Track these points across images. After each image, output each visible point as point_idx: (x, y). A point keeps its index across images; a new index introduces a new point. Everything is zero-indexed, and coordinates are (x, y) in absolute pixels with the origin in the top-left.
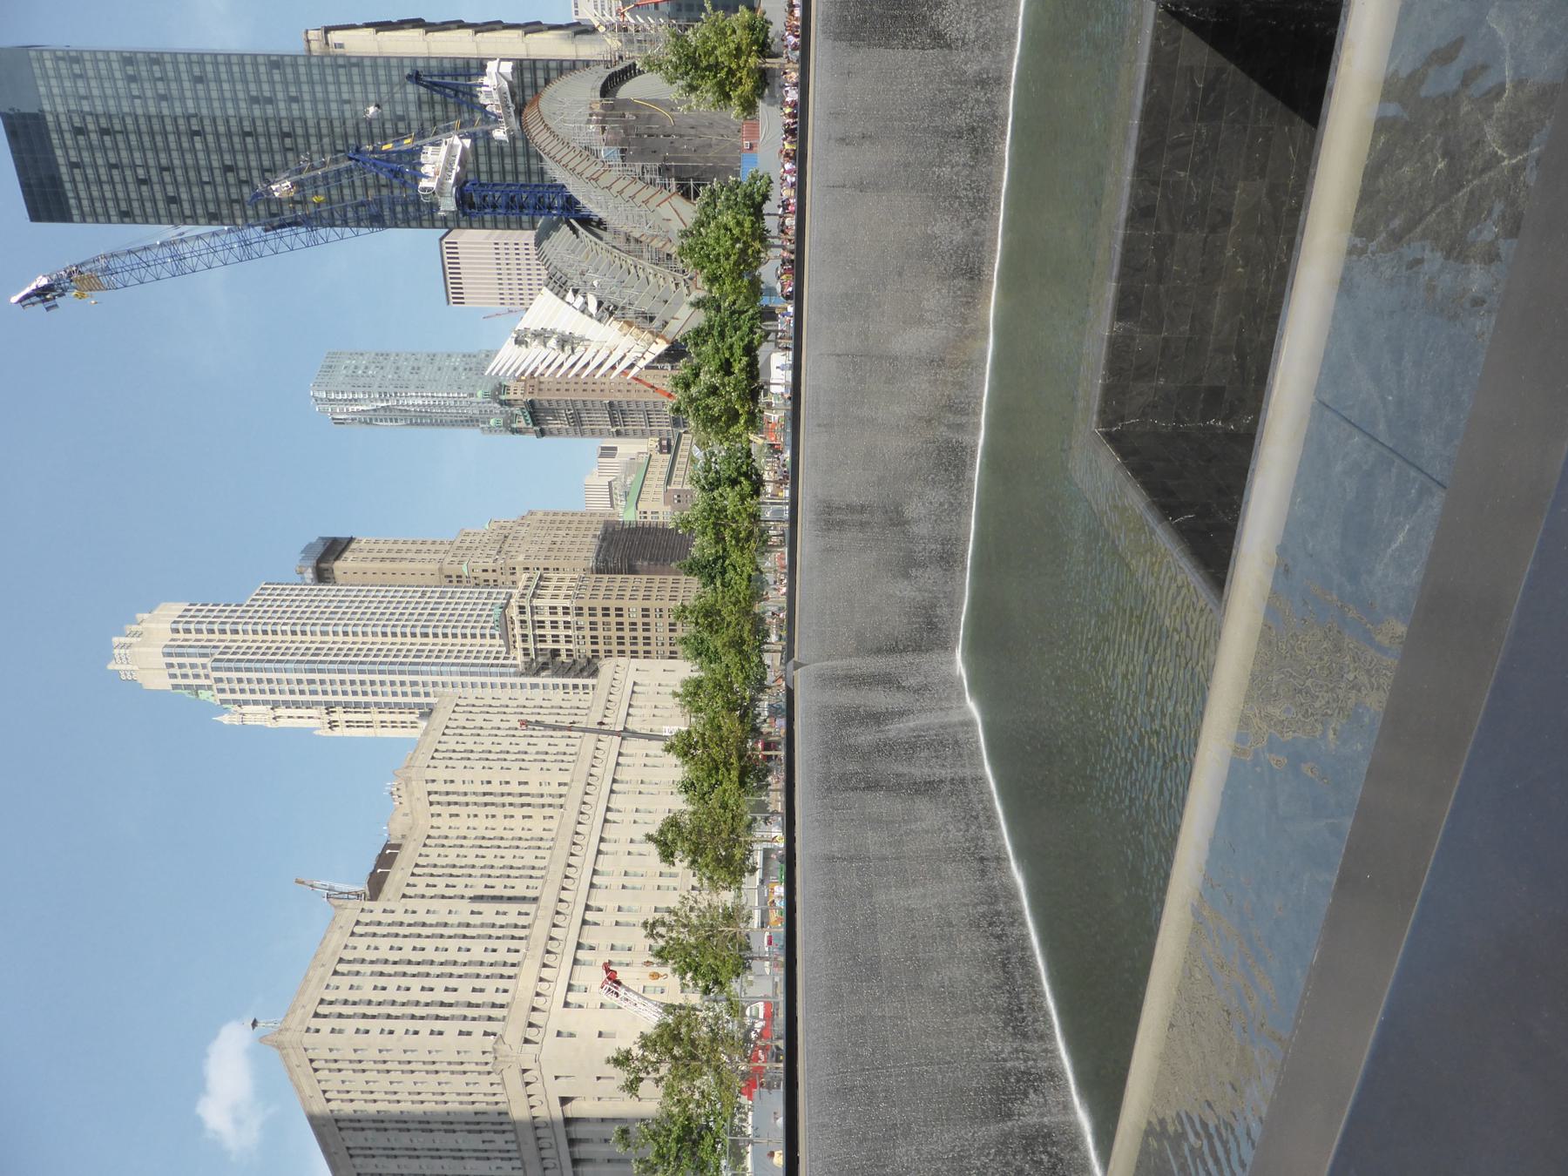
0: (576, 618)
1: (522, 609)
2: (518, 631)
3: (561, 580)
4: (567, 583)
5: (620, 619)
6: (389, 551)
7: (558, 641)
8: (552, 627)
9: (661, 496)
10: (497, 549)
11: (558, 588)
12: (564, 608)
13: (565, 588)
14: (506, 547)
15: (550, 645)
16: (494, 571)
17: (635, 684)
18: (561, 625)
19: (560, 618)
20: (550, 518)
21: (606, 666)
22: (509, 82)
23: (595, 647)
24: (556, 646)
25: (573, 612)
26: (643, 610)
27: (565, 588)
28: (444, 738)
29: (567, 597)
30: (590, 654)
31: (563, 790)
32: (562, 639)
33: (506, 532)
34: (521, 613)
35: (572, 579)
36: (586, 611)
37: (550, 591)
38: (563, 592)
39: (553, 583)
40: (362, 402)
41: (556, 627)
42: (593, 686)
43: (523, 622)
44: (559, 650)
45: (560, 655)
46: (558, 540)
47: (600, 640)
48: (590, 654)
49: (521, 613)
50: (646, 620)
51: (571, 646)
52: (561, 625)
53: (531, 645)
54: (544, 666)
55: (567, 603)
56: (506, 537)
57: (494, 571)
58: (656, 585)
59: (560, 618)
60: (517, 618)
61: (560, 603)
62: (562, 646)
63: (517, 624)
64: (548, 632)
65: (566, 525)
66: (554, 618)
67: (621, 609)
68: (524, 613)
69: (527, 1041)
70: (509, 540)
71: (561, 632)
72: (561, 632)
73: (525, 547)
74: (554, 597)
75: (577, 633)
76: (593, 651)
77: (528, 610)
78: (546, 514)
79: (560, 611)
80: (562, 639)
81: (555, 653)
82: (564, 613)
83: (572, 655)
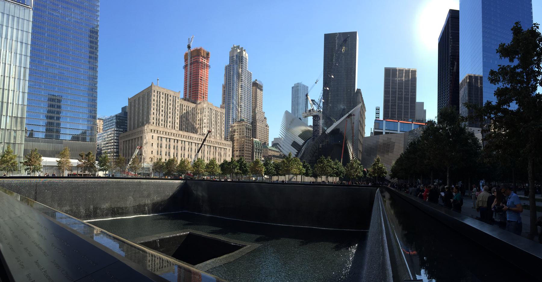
1: (243, 125)
6: (260, 98)
9: (271, 154)
14: (260, 121)
17: (226, 149)
20: (267, 130)
21: (230, 143)
26: (243, 150)
28: (215, 111)
33: (264, 121)
44: (235, 133)
50: (241, 151)
56: (263, 121)
58: (249, 153)
69: (151, 130)
70: (262, 122)
73: (261, 125)
74: (246, 132)
78: (268, 130)
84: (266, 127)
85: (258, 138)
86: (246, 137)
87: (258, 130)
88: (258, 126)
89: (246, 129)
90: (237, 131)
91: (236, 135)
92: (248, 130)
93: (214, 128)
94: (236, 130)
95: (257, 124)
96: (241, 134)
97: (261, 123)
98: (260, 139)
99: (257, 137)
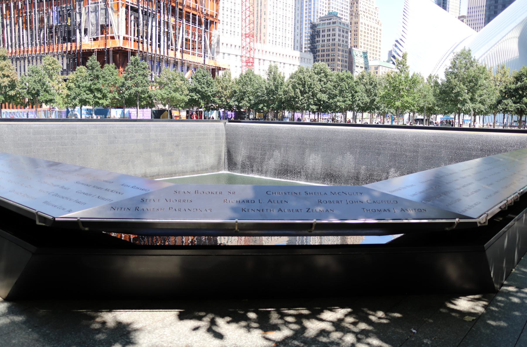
0: (321, 44)
1: (334, 23)
2: (327, 21)
3: (347, 37)
4: (345, 40)
5: (330, 60)
7: (323, 37)
8: (323, 35)
10: (366, 11)
11: (343, 36)
12: (335, 39)
13: (343, 39)
15: (321, 34)
16: (357, 10)
18: (328, 38)
19: (331, 38)
22: (75, 51)
23: (320, 51)
24: (321, 36)
25: (333, 42)
27: (343, 39)
29: (339, 40)
30: (318, 49)
31: (262, 41)
32: (323, 39)
34: (333, 22)
35: (347, 42)
36: (333, 47)
37: (342, 33)
38: (341, 39)
39: (345, 35)
40: (39, 15)
41: (328, 36)
42: (302, 51)
43: (330, 23)
45: (318, 38)
46: (369, 35)
47: (323, 53)
48: (318, 49)
49: (333, 22)
51: (321, 42)
52: (328, 38)
53: (321, 27)
54: (314, 31)
55: (337, 40)
57: (357, 10)
59: (331, 38)
60: (331, 21)
61: (337, 37)
62: (321, 39)
63: (329, 21)
64: (326, 33)
65: (376, 38)
66: (331, 35)
67: (334, 60)
68: (333, 24)
71: (326, 38)
72: (326, 38)
73: (367, 23)
74: (339, 35)
75: (331, 43)
76: (319, 50)
77: (334, 25)
79: (334, 37)
80: (323, 39)
81: (319, 36)
82: (323, 40)
83: (318, 42)
84: (376, 26)
85: (361, 47)
86: (339, 45)
87: (361, 31)
88: (362, 23)
89: (340, 30)
90: (323, 34)
91: (321, 42)
92: (343, 31)
93: (281, 29)
94: (321, 31)
95: (361, 20)
96: (331, 41)
97: (367, 17)
98: (364, 48)
99: (360, 44)
